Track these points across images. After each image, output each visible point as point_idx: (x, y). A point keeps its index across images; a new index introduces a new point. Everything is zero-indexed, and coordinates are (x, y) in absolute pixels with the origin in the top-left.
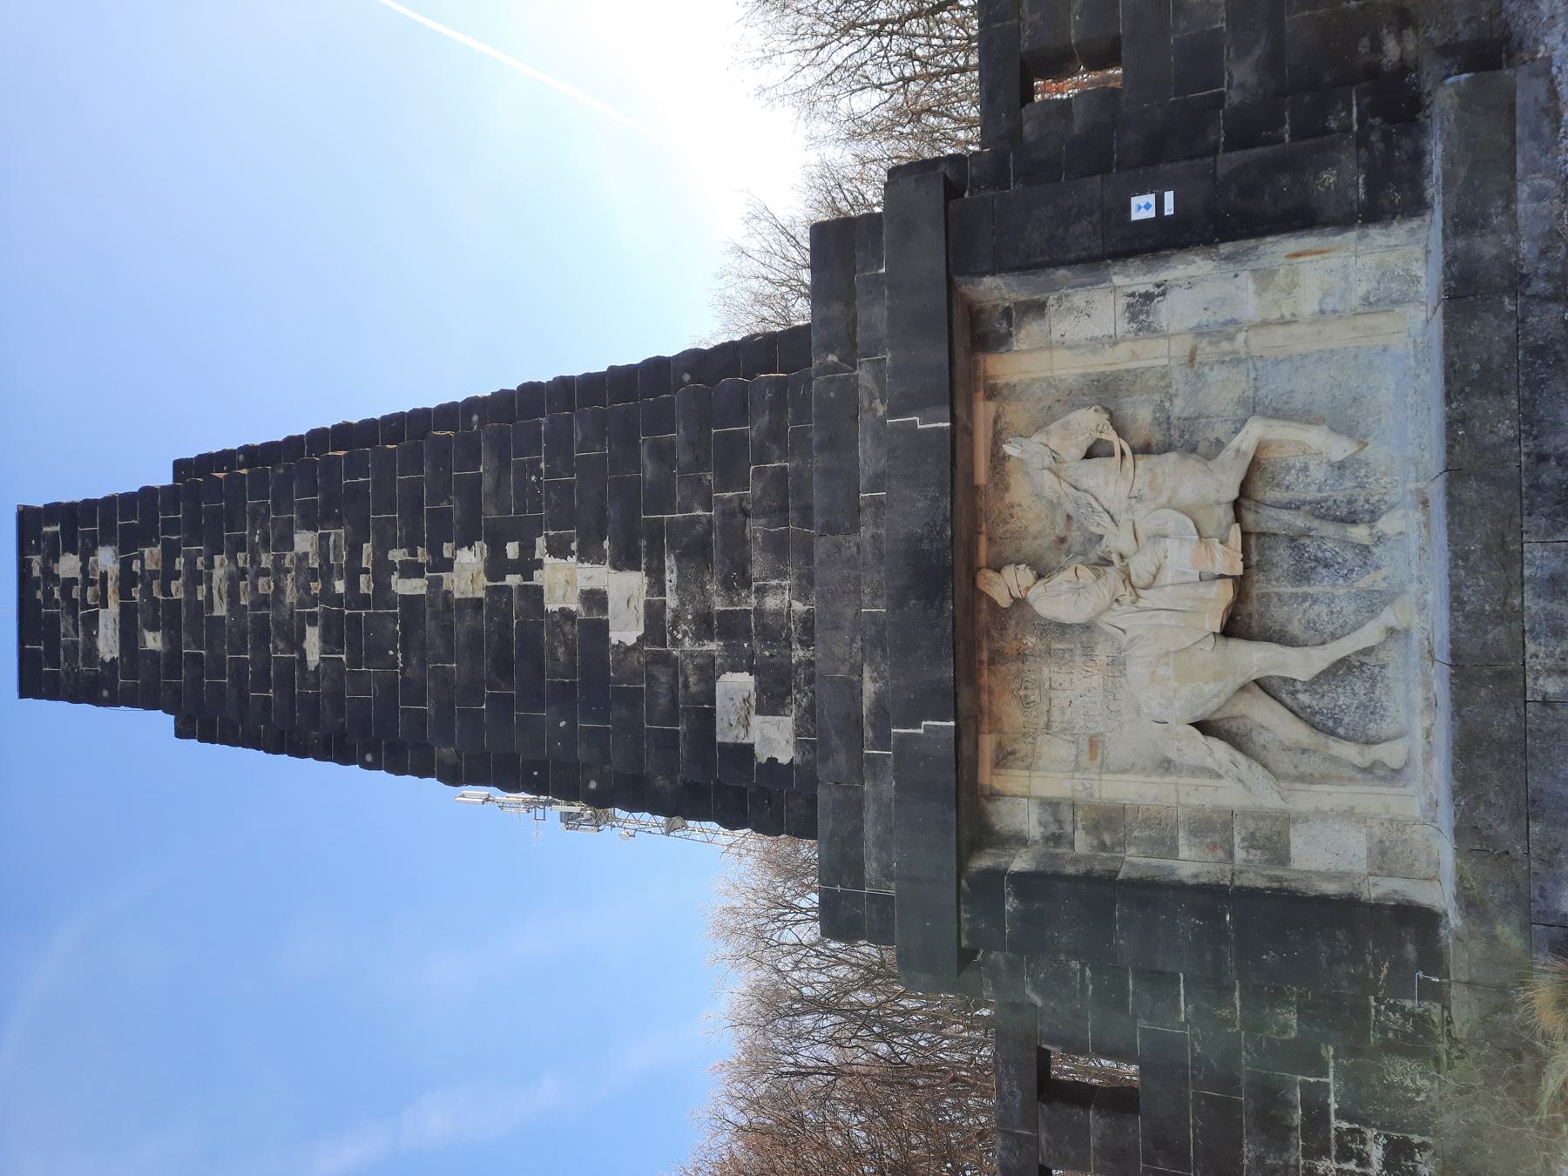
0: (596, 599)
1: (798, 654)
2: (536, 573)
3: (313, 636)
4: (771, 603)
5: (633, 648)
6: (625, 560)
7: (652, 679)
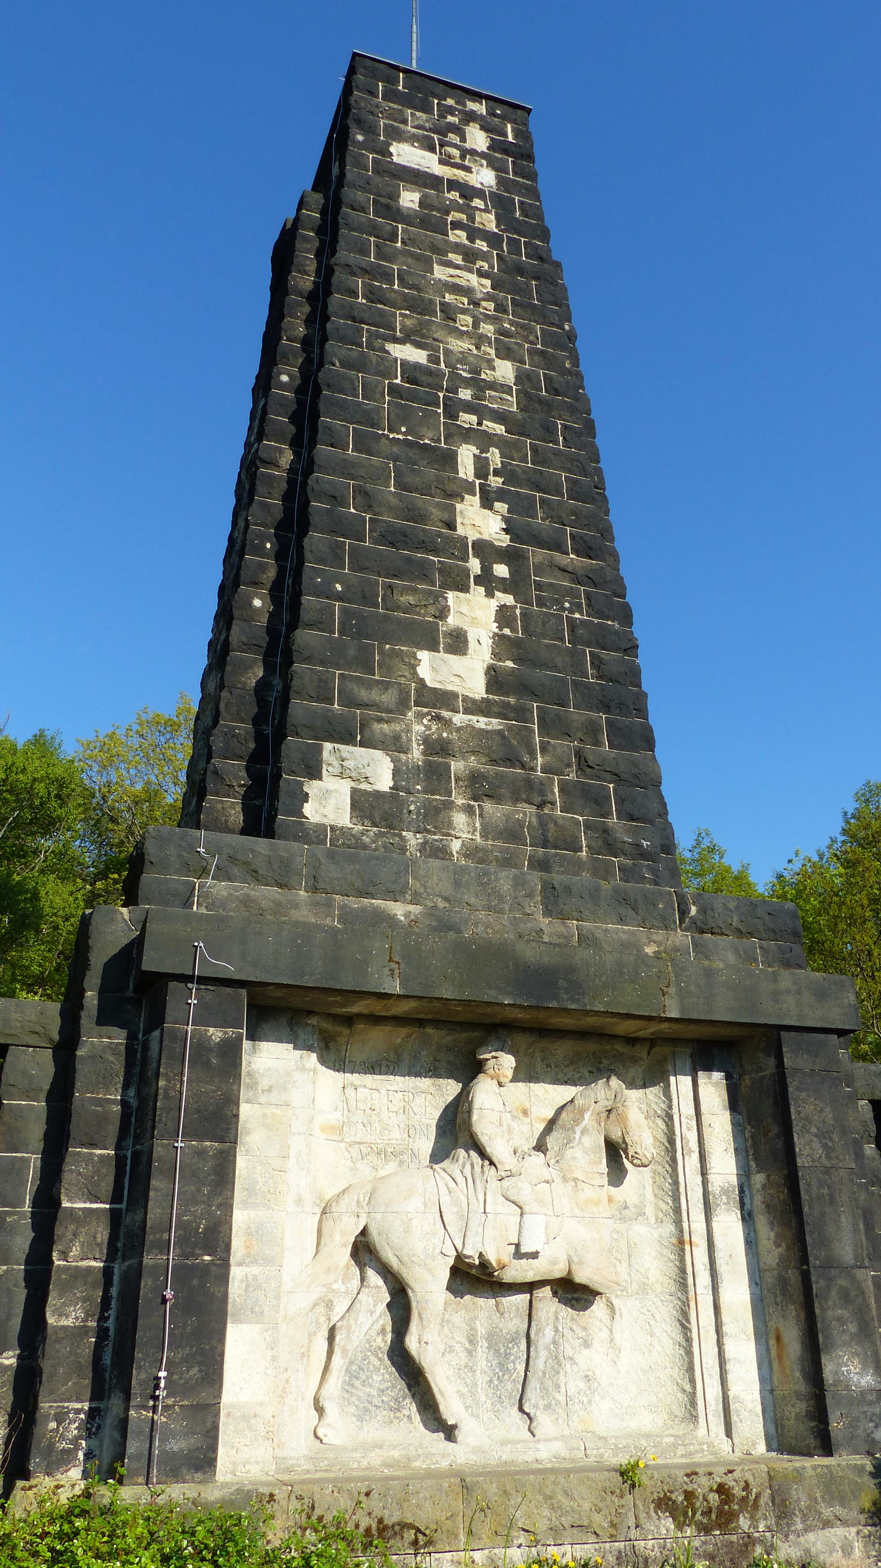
0: (458, 643)
2: (481, 590)
3: (419, 356)
4: (460, 819)
5: (415, 673)
6: (495, 679)
7: (386, 686)
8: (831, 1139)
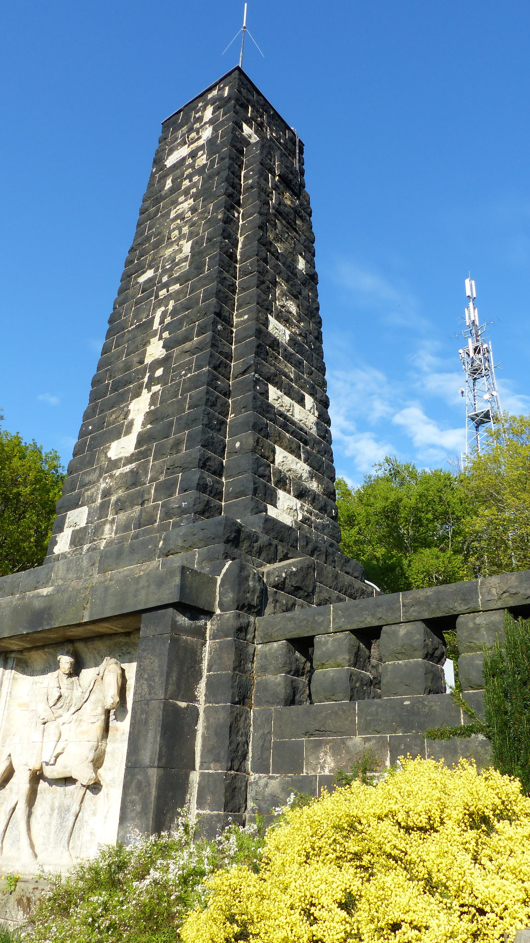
1: (86, 547)
5: (106, 456)
8: (154, 681)
